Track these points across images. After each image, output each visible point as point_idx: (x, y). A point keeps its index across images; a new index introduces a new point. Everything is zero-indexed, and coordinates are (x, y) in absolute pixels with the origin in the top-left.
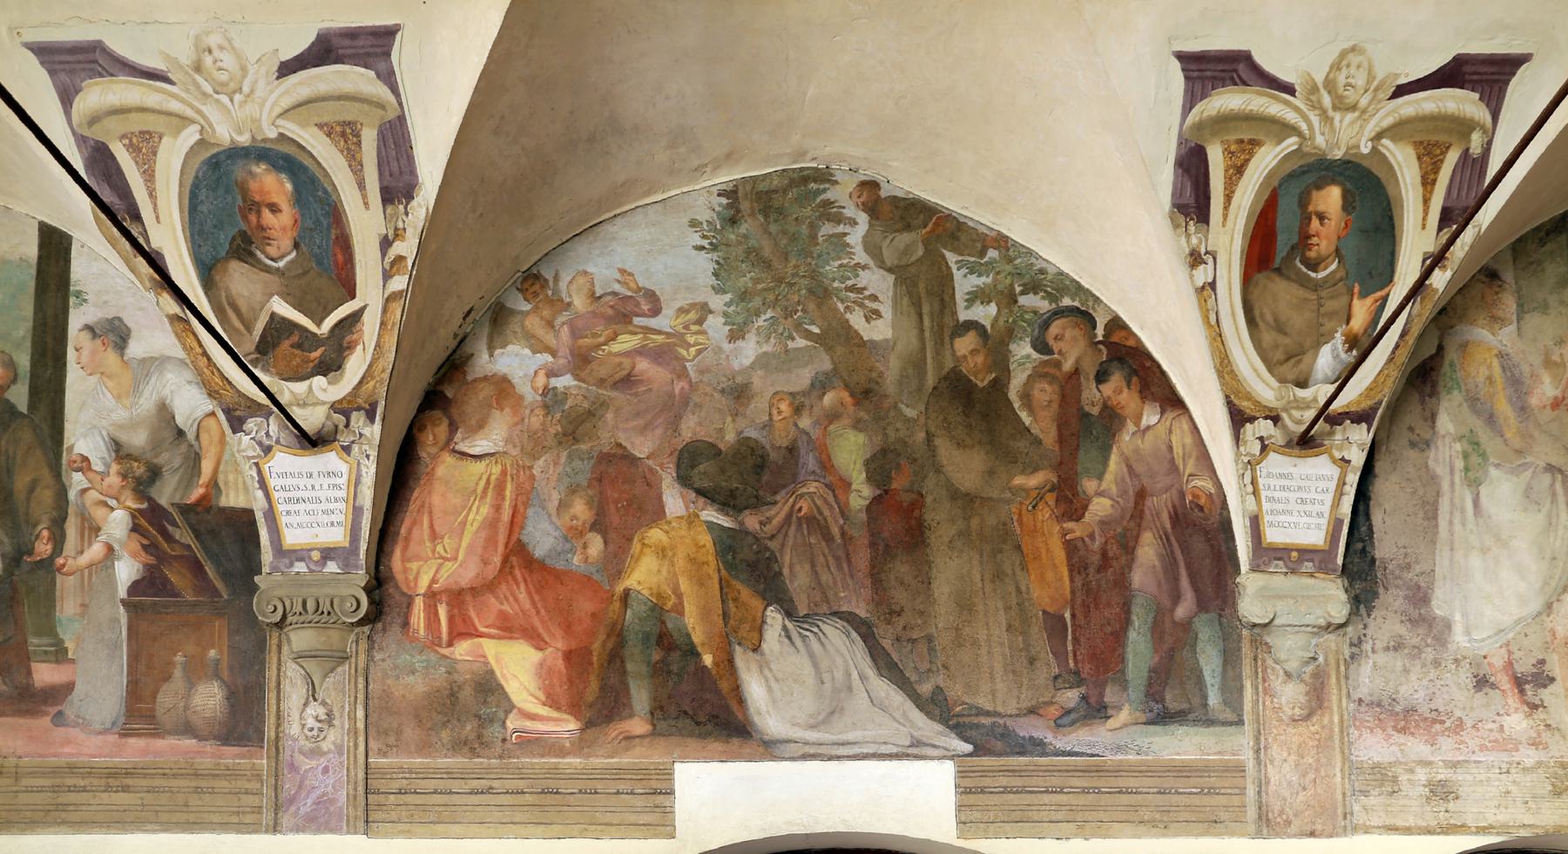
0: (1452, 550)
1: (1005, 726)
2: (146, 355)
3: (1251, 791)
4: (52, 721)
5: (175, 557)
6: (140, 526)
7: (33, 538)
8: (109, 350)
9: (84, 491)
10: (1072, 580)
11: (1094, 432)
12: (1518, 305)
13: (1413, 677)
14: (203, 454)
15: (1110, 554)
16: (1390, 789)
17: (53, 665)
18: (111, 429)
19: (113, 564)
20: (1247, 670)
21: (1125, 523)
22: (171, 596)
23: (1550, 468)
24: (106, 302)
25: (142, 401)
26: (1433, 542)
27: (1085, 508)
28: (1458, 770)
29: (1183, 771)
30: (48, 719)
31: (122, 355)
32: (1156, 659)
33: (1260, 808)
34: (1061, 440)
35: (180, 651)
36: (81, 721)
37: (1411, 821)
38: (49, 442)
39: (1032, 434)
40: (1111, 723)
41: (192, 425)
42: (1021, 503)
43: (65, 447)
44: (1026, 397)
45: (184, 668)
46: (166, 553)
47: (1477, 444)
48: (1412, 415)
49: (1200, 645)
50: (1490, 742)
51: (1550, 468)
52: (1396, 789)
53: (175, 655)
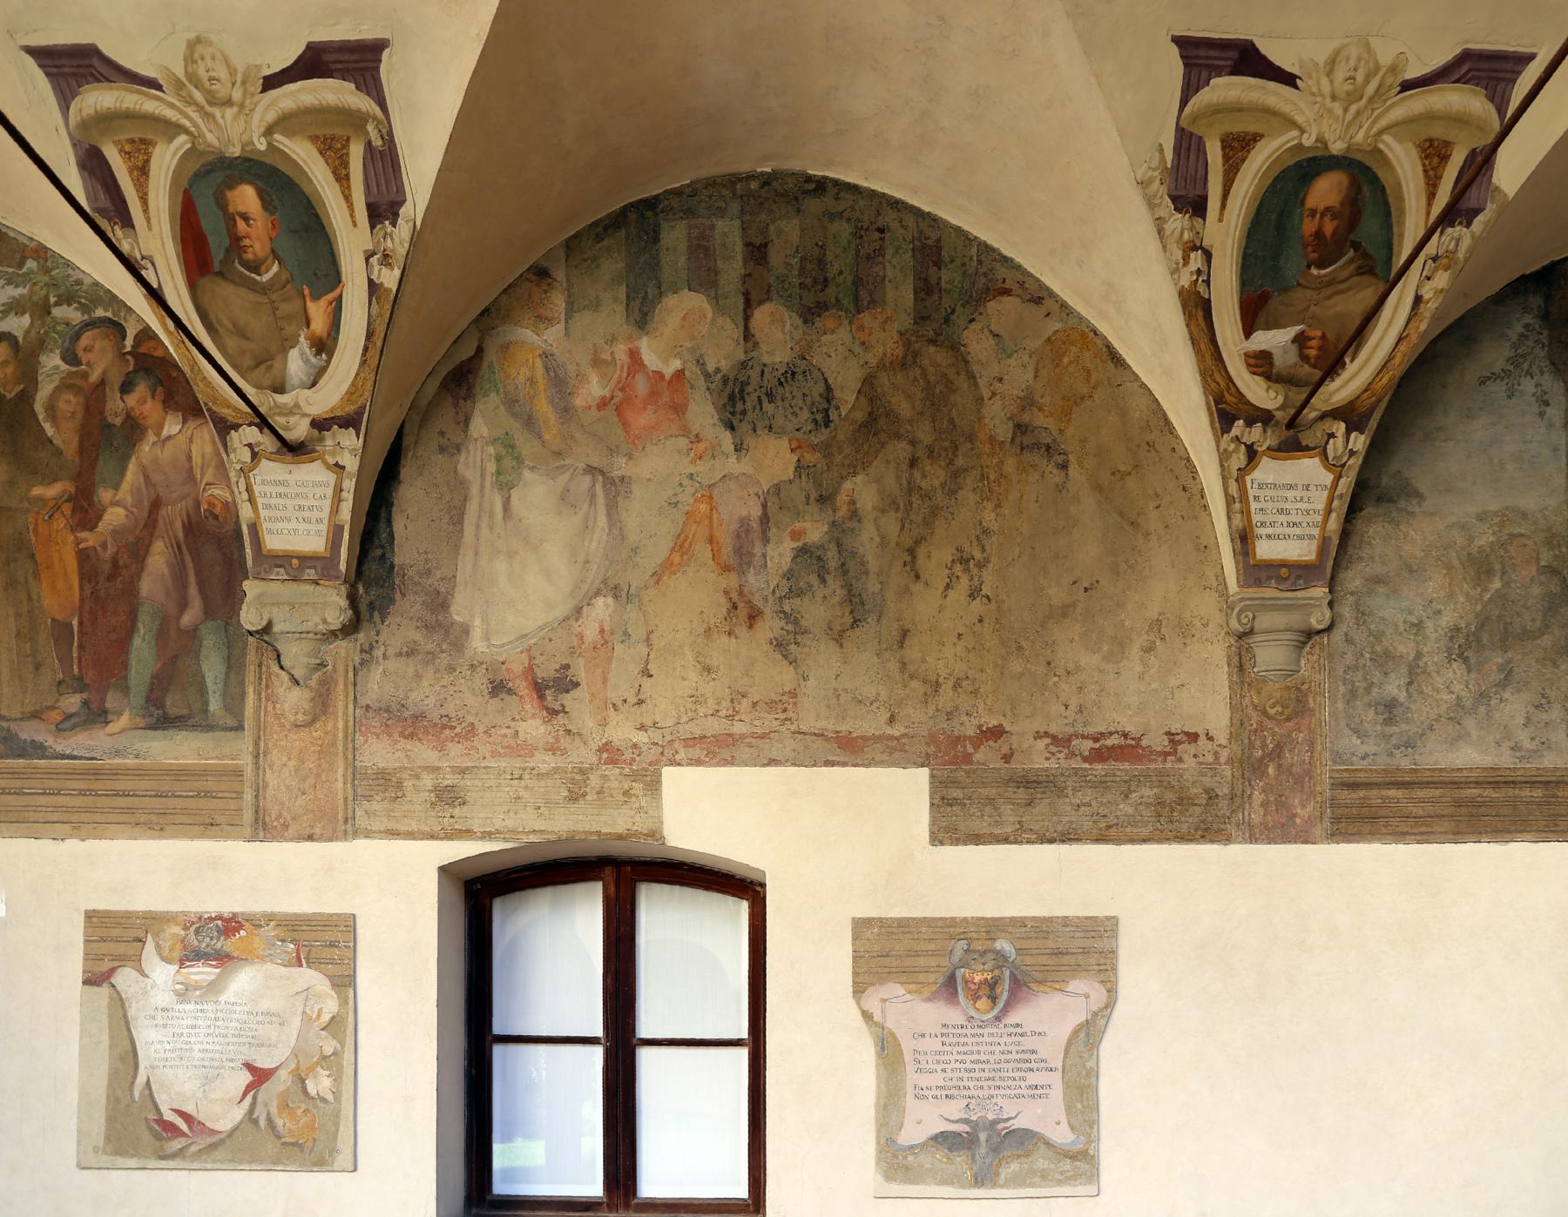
0: (476, 554)
1: (9, 730)
3: (248, 796)
10: (81, 588)
11: (115, 444)
12: (567, 303)
13: (425, 683)
15: (121, 563)
16: (393, 795)
20: (250, 676)
21: (137, 532)
23: (591, 470)
26: (457, 547)
27: (99, 518)
28: (466, 776)
29: (180, 773)
32: (159, 665)
33: (257, 812)
34: (81, 451)
37: (414, 826)
39: (54, 445)
40: (112, 728)
42: (38, 513)
44: (51, 409)
47: (512, 447)
48: (444, 419)
49: (204, 652)
50: (503, 747)
51: (591, 470)
52: (400, 794)
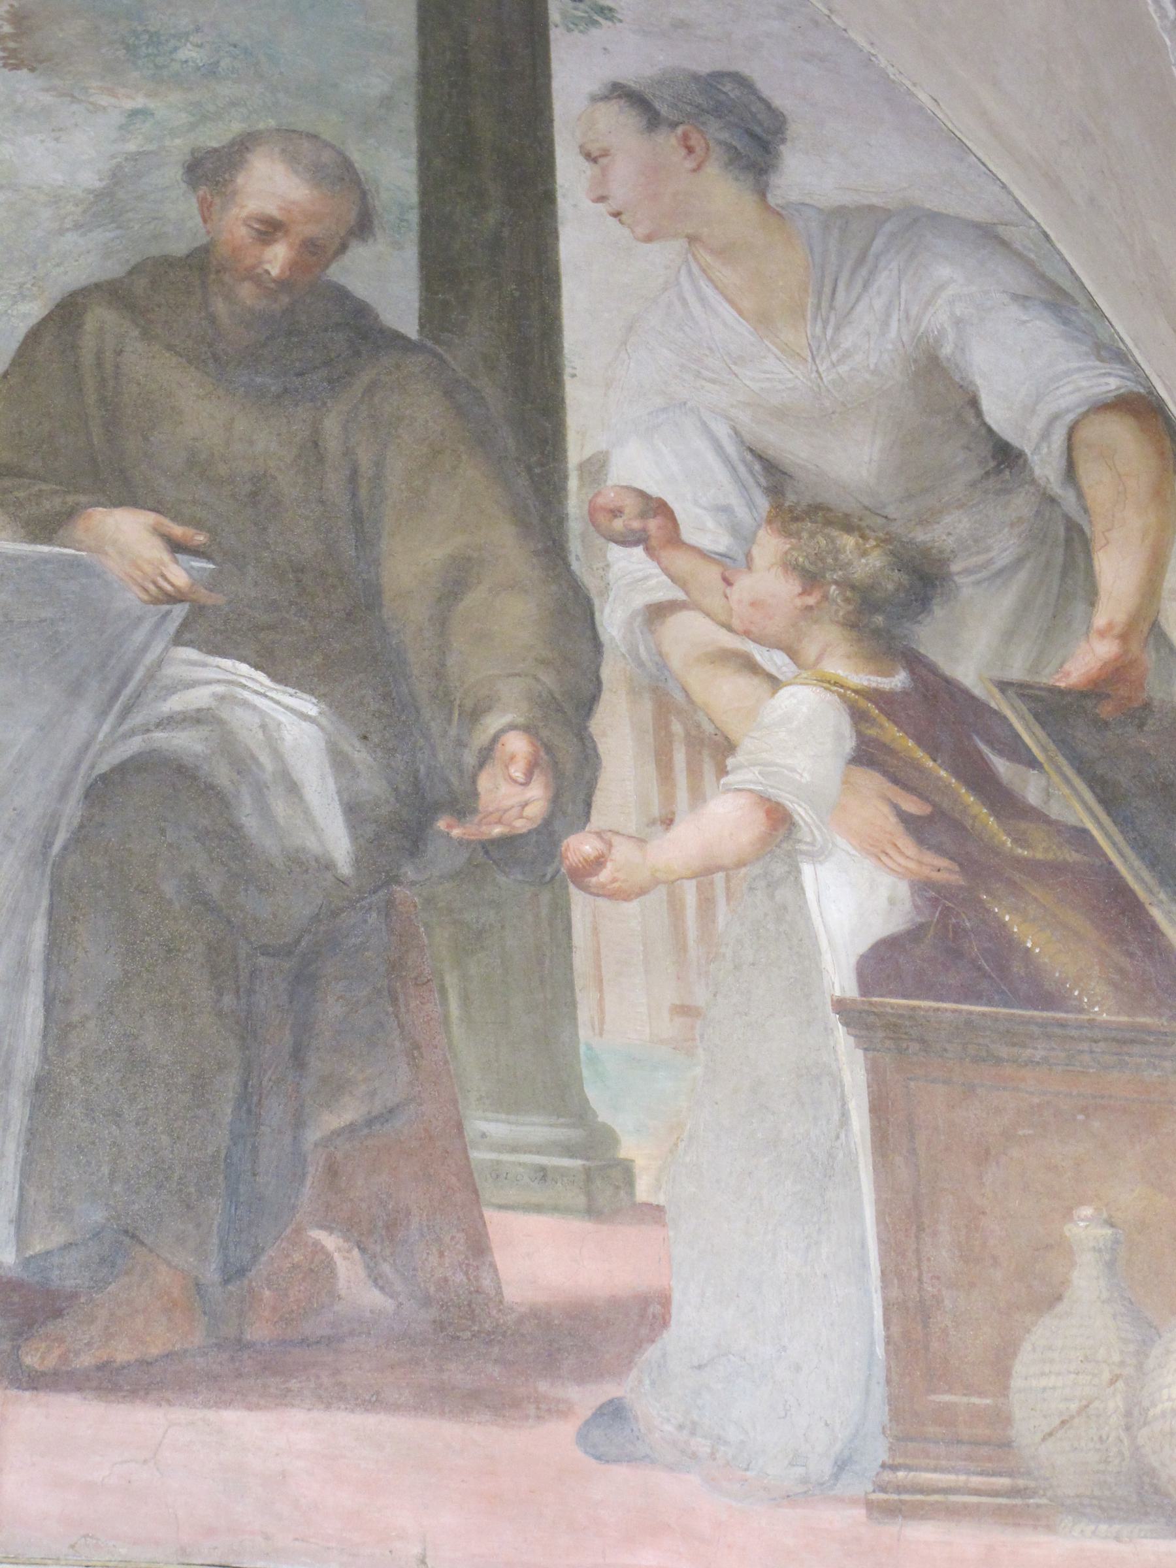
2: (847, 199)
4: (583, 1437)
5: (1034, 869)
6: (891, 752)
7: (470, 758)
8: (712, 169)
9: (657, 612)
14: (1096, 529)
17: (579, 1225)
18: (744, 417)
19: (796, 871)
22: (1029, 1002)
24: (680, 25)
25: (849, 338)
30: (563, 1431)
31: (762, 192)
35: (1081, 1202)
36: (702, 1446)
38: (507, 439)
41: (1045, 435)
43: (576, 453)
45: (1111, 1265)
46: (996, 851)
53: (1068, 1215)
